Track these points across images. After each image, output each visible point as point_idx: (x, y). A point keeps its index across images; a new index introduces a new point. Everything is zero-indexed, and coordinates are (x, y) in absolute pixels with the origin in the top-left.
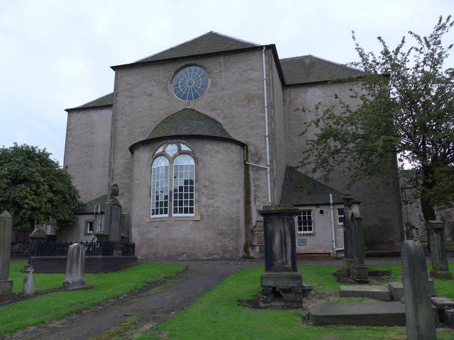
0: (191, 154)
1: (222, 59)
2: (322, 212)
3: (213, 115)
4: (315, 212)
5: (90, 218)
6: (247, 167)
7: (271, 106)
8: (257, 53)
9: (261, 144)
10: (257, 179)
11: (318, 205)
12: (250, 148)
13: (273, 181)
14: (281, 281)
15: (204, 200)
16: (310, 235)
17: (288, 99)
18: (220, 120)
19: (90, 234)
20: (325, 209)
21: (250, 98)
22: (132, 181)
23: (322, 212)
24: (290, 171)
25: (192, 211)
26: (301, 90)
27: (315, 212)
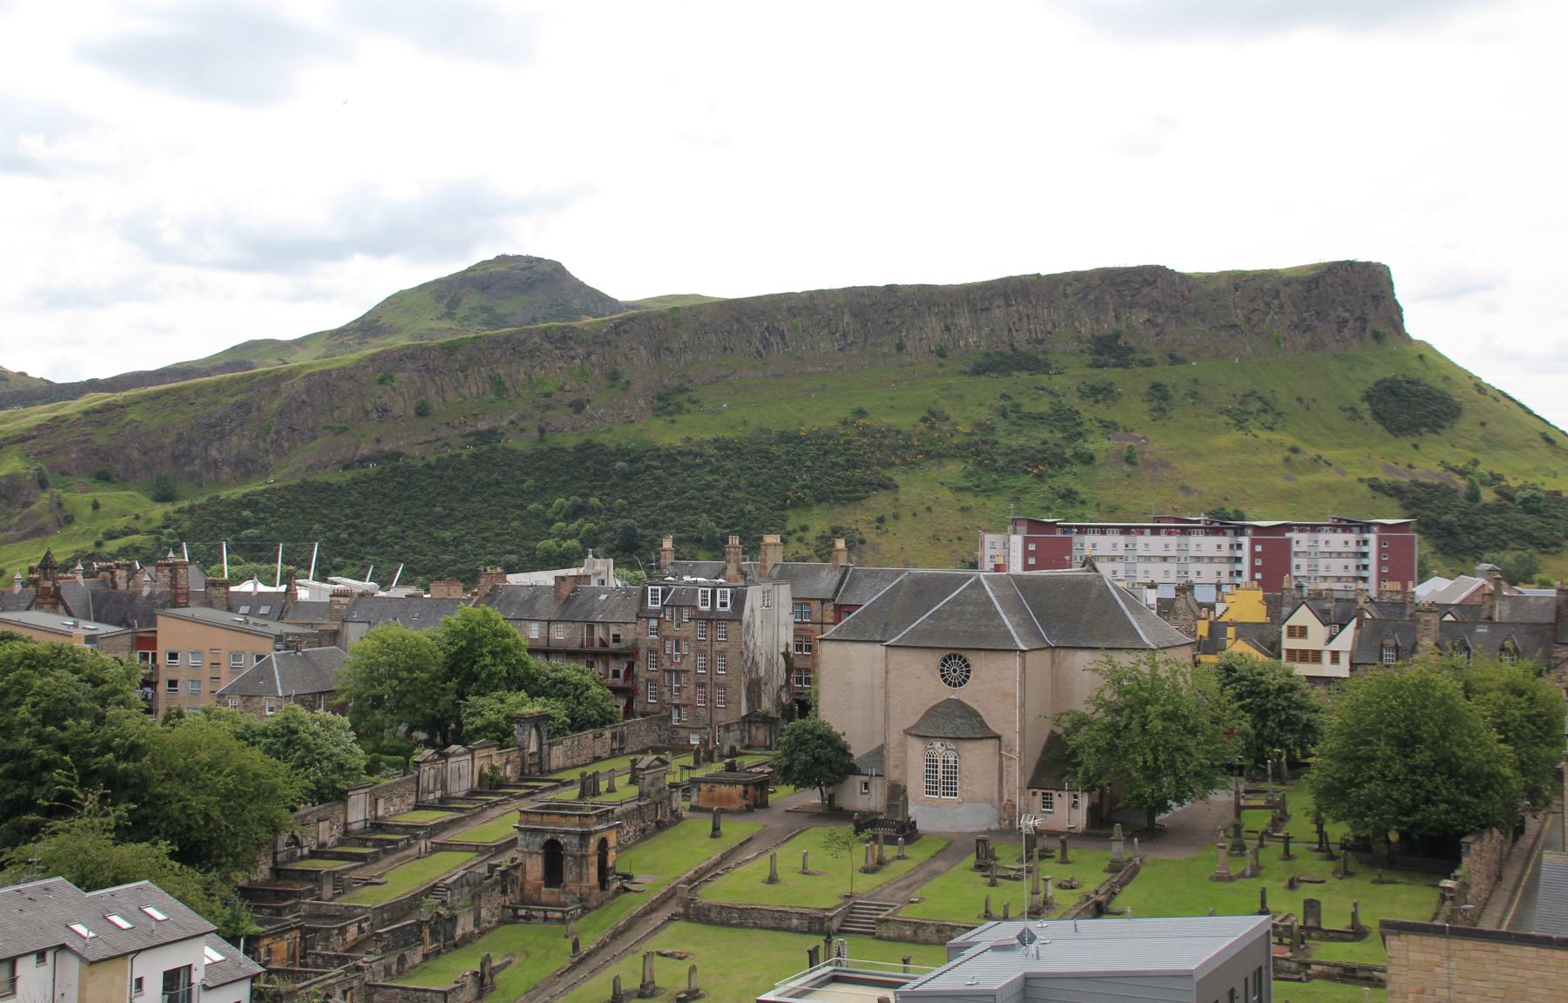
0: (956, 751)
1: (983, 653)
2: (1060, 796)
3: (974, 706)
4: (1055, 794)
5: (865, 779)
6: (1001, 754)
7: (1023, 705)
8: (1012, 653)
9: (1012, 734)
10: (1008, 766)
11: (1057, 790)
12: (1003, 739)
13: (1022, 769)
14: (981, 862)
15: (965, 787)
16: (1050, 812)
17: (1057, 660)
18: (980, 711)
19: (865, 793)
20: (1062, 793)
21: (1006, 695)
22: (906, 755)
23: (1060, 796)
24: (1053, 741)
25: (955, 795)
26: (1071, 652)
27: (1055, 794)
